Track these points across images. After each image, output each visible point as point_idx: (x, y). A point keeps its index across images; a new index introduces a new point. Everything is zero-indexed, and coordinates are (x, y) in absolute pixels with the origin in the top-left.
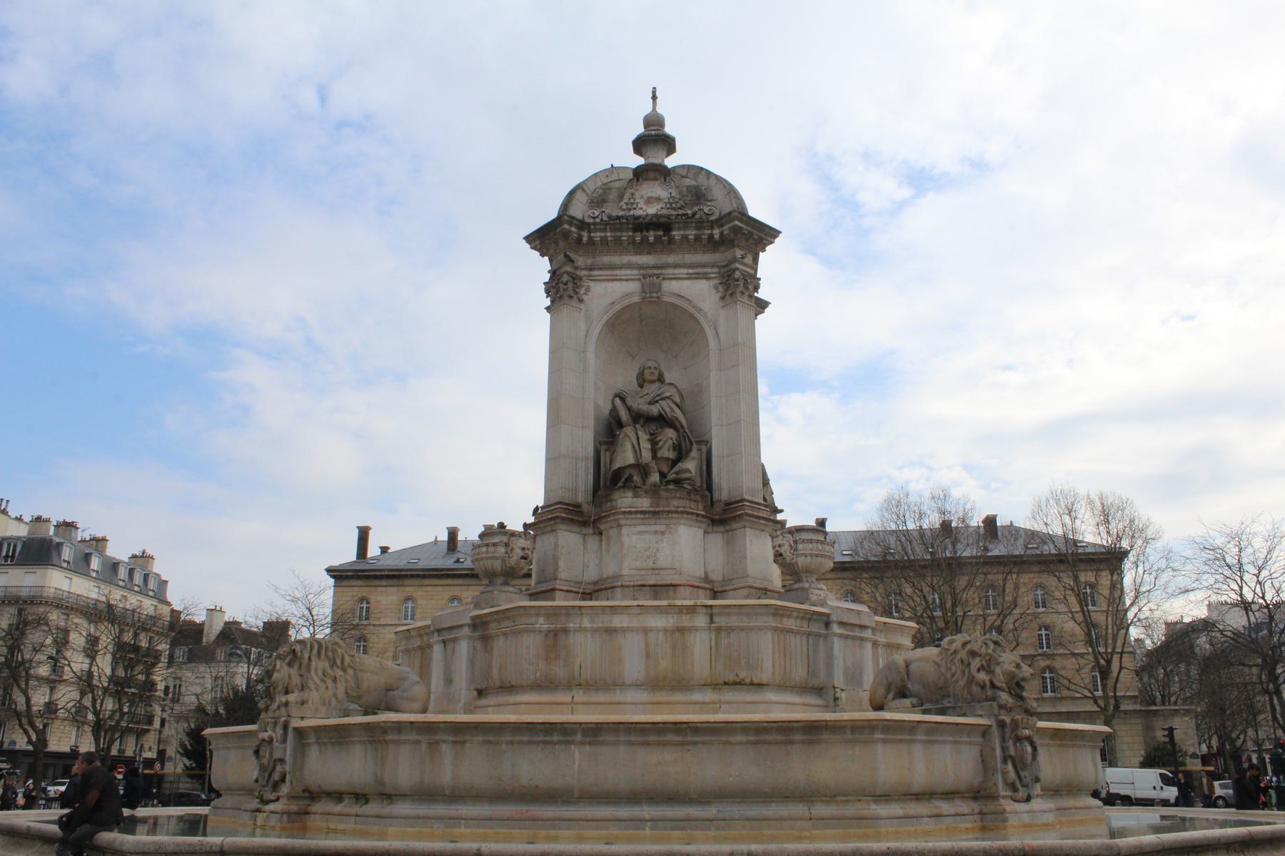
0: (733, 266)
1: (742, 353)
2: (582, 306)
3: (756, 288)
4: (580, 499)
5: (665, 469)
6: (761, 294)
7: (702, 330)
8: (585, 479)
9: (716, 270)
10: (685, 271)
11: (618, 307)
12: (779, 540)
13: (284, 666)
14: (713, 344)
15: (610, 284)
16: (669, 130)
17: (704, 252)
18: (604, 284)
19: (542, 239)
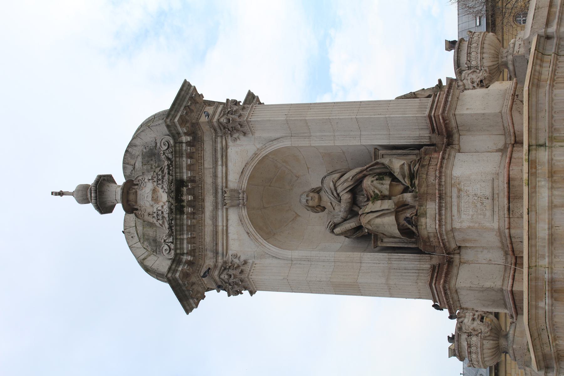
0: (216, 124)
1: (297, 116)
2: (250, 261)
3: (236, 103)
4: (427, 266)
5: (400, 188)
6: (241, 98)
7: (275, 153)
8: (409, 261)
9: (219, 140)
10: (220, 168)
11: (252, 229)
12: (468, 83)
14: (287, 143)
15: (230, 235)
16: (90, 181)
17: (203, 150)
18: (231, 242)
19: (188, 298)
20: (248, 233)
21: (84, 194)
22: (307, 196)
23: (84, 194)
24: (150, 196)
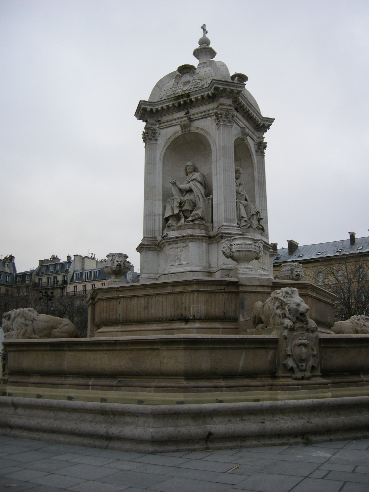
10: (200, 115)
11: (172, 139)
13: (6, 320)
18: (166, 130)
20: (170, 138)
21: (204, 42)
22: (191, 165)
23: (204, 42)
24: (186, 81)
